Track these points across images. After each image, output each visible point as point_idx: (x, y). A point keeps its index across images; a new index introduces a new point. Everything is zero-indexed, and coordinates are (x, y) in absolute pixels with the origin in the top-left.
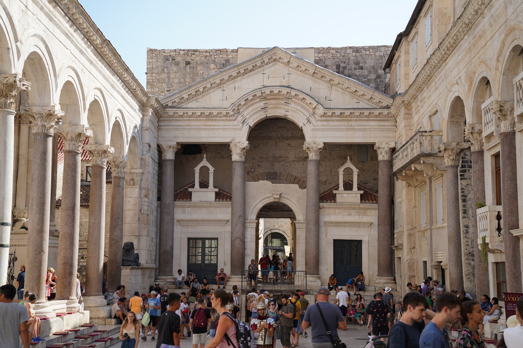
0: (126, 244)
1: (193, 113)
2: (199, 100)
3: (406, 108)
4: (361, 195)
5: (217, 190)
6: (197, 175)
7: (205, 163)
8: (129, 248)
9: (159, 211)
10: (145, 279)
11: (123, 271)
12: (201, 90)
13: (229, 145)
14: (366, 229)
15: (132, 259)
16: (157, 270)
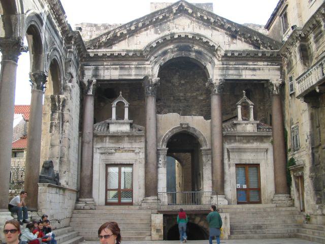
0: (45, 163)
1: (111, 54)
2: (117, 45)
3: (300, 41)
4: (258, 125)
5: (131, 121)
6: (114, 110)
7: (121, 99)
8: (48, 166)
9: (80, 141)
10: (66, 200)
11: (39, 188)
12: (118, 35)
13: (141, 84)
14: (263, 154)
15: (50, 177)
16: (78, 193)
